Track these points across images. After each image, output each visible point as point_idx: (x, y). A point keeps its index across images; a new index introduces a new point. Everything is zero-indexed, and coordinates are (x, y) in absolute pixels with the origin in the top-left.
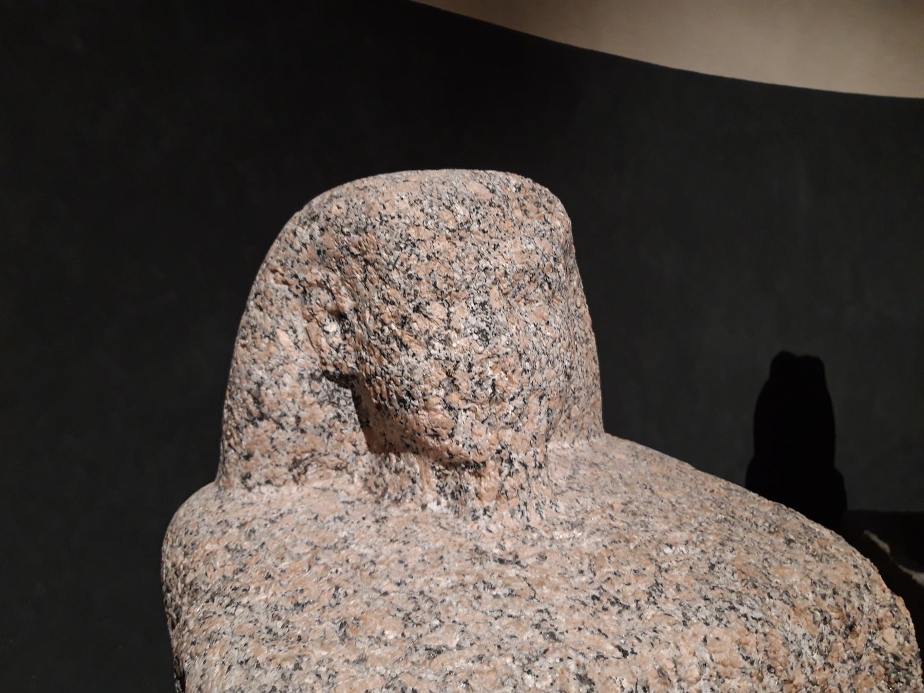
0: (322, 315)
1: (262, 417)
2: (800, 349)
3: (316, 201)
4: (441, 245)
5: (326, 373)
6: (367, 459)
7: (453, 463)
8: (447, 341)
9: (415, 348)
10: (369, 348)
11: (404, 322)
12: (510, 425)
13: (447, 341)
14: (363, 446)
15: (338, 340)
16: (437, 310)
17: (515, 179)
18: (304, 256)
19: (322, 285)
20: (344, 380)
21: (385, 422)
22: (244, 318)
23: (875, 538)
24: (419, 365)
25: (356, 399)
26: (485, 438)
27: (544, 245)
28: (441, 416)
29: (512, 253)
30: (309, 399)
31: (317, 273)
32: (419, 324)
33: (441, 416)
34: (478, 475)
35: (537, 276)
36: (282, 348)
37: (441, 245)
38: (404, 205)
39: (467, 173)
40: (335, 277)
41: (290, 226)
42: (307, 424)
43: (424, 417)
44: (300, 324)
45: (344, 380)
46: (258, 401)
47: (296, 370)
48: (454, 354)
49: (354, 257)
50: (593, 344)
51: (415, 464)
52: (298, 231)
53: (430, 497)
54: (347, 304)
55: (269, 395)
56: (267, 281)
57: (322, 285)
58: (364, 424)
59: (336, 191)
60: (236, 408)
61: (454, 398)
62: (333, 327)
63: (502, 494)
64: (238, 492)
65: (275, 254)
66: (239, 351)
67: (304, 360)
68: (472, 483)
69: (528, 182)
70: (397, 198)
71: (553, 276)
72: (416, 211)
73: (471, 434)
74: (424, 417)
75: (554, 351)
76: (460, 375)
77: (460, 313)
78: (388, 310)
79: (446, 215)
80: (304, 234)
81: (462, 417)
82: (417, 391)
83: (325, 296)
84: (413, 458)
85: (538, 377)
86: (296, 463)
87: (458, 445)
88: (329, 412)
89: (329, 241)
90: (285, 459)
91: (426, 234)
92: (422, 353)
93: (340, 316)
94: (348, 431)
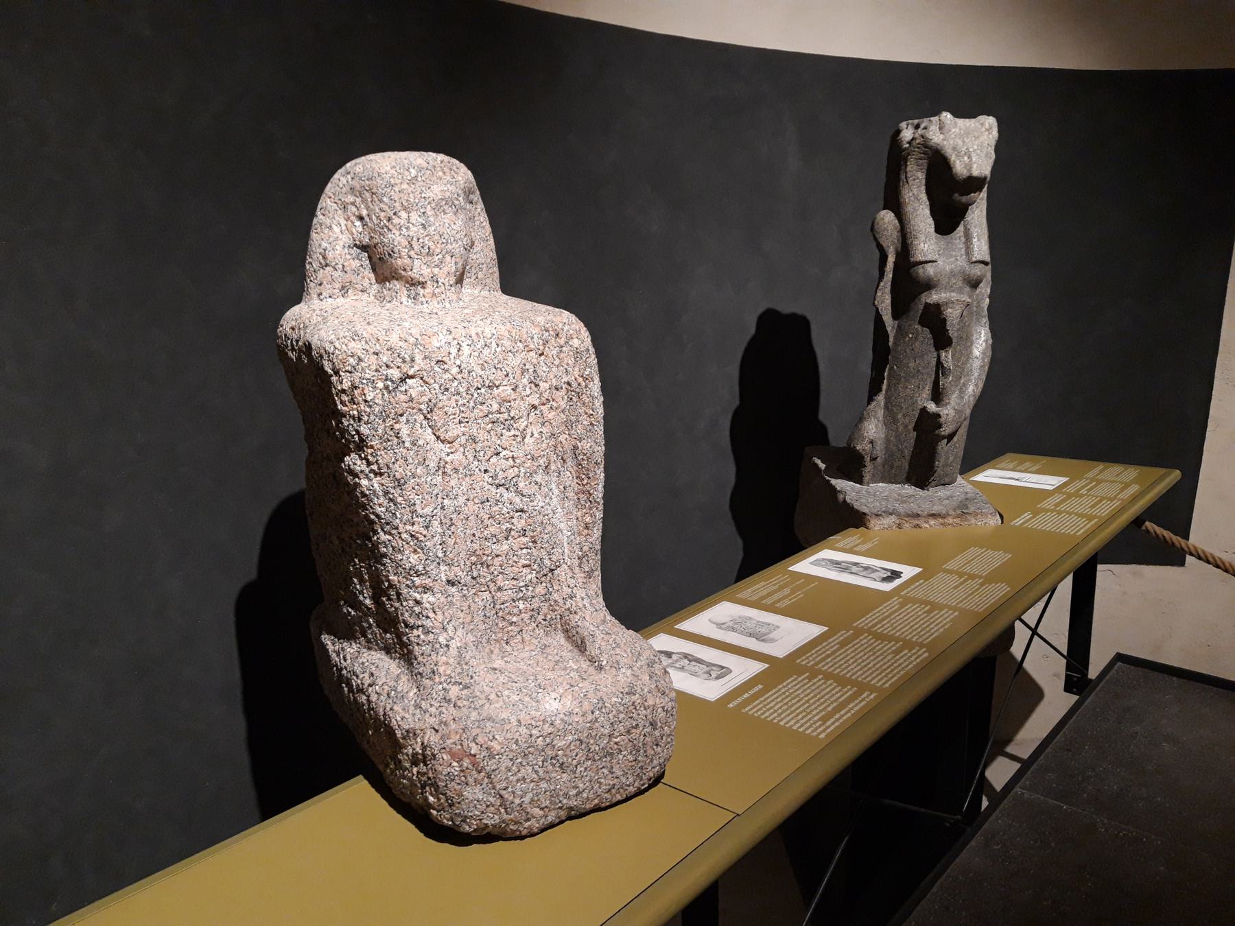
0: (353, 218)
1: (327, 265)
2: (786, 308)
3: (348, 165)
4: (405, 186)
5: (355, 245)
6: (376, 287)
7: (413, 283)
8: (408, 228)
9: (394, 231)
10: (374, 231)
11: (389, 219)
12: (437, 266)
13: (408, 228)
14: (374, 281)
15: (360, 229)
16: (403, 214)
17: (441, 157)
18: (344, 190)
19: (353, 204)
20: (364, 248)
21: (383, 267)
22: (315, 221)
23: (818, 462)
24: (396, 239)
25: (370, 257)
26: (426, 271)
27: (452, 188)
28: (407, 261)
29: (436, 191)
30: (348, 257)
31: (350, 198)
32: (396, 220)
33: (407, 261)
34: (424, 288)
35: (449, 202)
36: (333, 233)
37: (405, 186)
38: (388, 168)
39: (417, 154)
40: (358, 200)
41: (336, 176)
42: (347, 269)
43: (399, 262)
44: (343, 222)
45: (364, 248)
46: (324, 258)
47: (342, 243)
48: (411, 234)
49: (367, 191)
50: (492, 241)
51: (396, 285)
52: (340, 179)
53: (404, 299)
54: (364, 213)
55: (330, 255)
56: (326, 202)
57: (353, 204)
58: (374, 270)
59: (358, 160)
60: (313, 262)
61: (412, 253)
62: (358, 223)
63: (434, 295)
64: (316, 301)
65: (329, 189)
66: (313, 235)
67: (345, 239)
68: (421, 291)
69: (446, 158)
70: (386, 166)
71: (456, 202)
72: (393, 171)
73: (420, 269)
74: (399, 262)
75: (458, 236)
76: (414, 243)
77: (414, 217)
78: (383, 214)
79: (406, 173)
80: (344, 180)
81: (416, 262)
82: (396, 250)
83: (354, 209)
84: (396, 282)
85: (450, 247)
86: (343, 287)
87: (414, 274)
88: (357, 263)
89: (355, 183)
90: (338, 286)
91: (398, 181)
92: (397, 233)
93: (361, 218)
94: (367, 273)
